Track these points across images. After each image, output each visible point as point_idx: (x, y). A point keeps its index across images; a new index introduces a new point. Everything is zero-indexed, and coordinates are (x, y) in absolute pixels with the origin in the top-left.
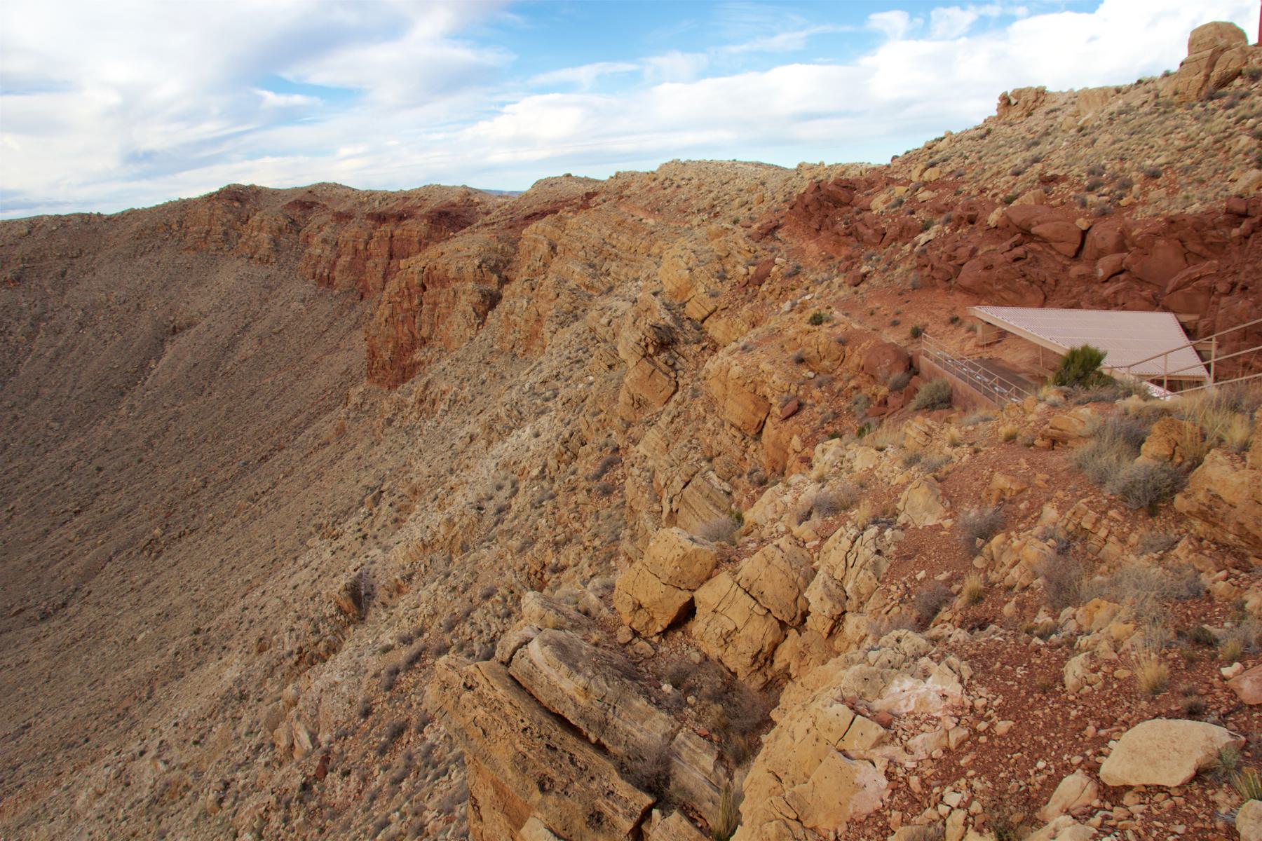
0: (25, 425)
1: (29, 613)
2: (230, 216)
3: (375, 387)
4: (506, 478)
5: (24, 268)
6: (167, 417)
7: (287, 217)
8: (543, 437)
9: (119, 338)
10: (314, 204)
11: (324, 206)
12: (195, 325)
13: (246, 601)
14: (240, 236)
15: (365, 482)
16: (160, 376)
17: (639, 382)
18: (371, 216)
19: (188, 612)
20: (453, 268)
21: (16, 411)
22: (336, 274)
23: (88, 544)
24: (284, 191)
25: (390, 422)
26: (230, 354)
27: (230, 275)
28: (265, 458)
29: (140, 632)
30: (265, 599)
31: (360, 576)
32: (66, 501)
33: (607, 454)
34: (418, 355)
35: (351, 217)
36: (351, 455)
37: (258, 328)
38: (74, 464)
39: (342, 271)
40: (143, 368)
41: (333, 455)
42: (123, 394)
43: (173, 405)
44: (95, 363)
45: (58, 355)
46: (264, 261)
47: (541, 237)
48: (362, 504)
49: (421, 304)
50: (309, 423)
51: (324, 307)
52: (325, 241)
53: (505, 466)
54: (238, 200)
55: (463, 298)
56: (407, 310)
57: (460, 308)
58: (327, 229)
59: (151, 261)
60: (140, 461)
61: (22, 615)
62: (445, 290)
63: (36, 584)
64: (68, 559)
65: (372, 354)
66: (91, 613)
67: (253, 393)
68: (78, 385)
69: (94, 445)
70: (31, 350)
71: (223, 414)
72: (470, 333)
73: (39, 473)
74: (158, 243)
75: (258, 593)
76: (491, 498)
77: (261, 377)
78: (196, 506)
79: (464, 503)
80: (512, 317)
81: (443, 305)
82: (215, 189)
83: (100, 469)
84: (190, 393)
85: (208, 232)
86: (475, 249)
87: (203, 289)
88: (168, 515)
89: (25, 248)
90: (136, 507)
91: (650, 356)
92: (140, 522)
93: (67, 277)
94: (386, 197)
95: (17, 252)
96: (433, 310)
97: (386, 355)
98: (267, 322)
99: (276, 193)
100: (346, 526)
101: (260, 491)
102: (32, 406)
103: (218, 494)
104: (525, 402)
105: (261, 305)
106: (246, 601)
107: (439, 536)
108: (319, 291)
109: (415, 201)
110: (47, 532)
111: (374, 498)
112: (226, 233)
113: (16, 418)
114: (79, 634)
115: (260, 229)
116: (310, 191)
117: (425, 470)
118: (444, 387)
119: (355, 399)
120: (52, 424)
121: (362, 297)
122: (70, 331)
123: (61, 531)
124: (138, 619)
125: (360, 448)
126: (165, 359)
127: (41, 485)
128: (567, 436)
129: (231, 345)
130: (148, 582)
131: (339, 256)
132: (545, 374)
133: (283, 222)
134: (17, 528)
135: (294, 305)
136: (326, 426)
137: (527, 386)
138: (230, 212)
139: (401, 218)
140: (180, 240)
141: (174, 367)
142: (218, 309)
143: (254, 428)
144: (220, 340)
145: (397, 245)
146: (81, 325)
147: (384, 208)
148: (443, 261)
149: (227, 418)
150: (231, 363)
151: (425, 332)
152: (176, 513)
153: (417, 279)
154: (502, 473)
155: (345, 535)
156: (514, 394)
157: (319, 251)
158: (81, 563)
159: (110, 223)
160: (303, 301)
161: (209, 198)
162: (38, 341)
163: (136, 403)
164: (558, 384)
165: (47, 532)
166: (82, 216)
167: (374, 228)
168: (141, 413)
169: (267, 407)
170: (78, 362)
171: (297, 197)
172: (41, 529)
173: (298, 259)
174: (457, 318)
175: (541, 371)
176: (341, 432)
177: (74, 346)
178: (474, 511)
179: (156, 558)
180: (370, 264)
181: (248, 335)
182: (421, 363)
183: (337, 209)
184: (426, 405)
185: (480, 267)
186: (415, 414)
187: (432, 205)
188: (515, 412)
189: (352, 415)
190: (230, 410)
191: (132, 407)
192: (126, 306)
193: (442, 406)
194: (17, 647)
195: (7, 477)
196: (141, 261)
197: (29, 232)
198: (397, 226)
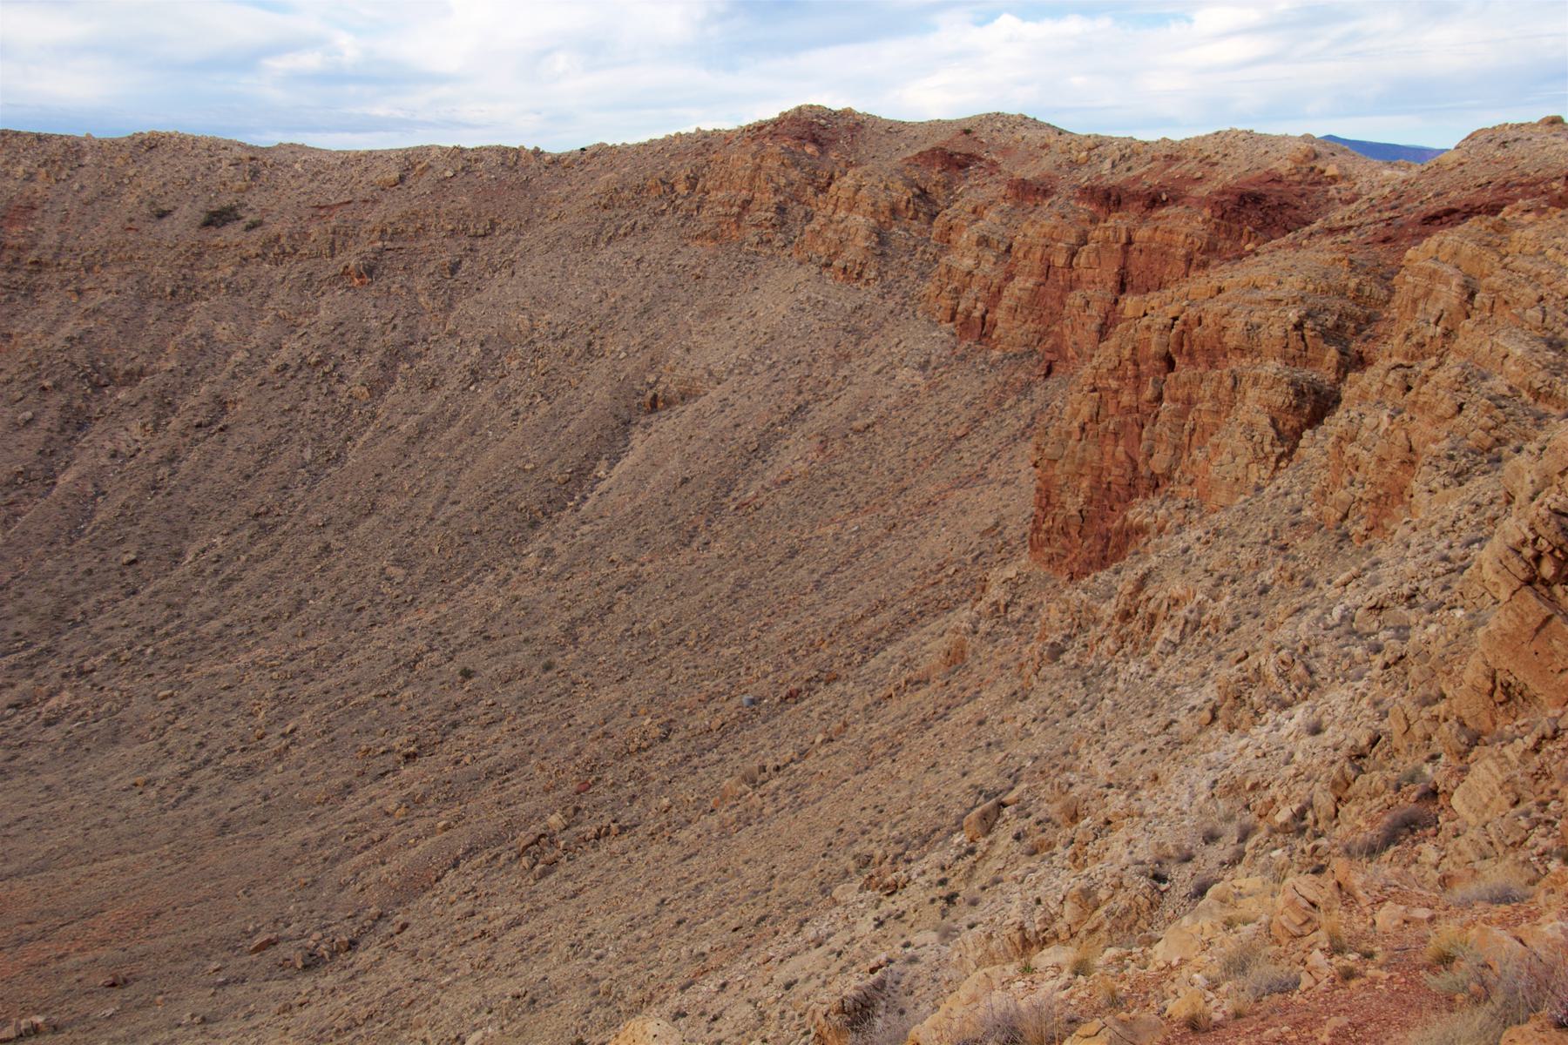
0: (342, 566)
1: (284, 951)
2: (795, 174)
3: (1042, 571)
4: (1229, 818)
5: (384, 250)
6: (613, 583)
7: (911, 183)
8: (1327, 737)
9: (544, 409)
10: (971, 158)
11: (993, 164)
12: (697, 396)
13: (686, 999)
14: (809, 217)
15: (977, 778)
16: (613, 496)
17: (1508, 640)
18: (1089, 193)
19: (575, 1001)
20: (1238, 324)
21: (329, 535)
22: (1000, 314)
23: (420, 826)
24: (912, 126)
25: (1056, 652)
26: (758, 466)
27: (780, 296)
28: (795, 695)
29: (475, 1028)
30: (723, 1000)
31: (880, 985)
32: (393, 731)
33: (1407, 803)
34: (1138, 513)
35: (1046, 193)
36: (965, 713)
37: (822, 416)
38: (419, 657)
39: (1013, 311)
40: (581, 476)
41: (929, 709)
42: (535, 525)
43: (630, 560)
44: (490, 456)
45: (422, 432)
46: (851, 274)
47: (1448, 269)
48: (959, 826)
49: (1159, 398)
50: (897, 630)
51: (966, 385)
52: (984, 241)
53: (1233, 789)
54: (815, 140)
55: (1252, 393)
56: (1129, 410)
57: (1243, 416)
58: (991, 215)
59: (625, 255)
60: (548, 667)
61: (271, 953)
62: (1214, 373)
63: (310, 893)
64: (375, 850)
65: (1046, 498)
66: (397, 971)
67: (793, 553)
68: (452, 496)
69: (464, 623)
70: (374, 417)
71: (726, 591)
72: (1258, 473)
73: (352, 666)
74: (644, 219)
75: (710, 985)
76: (1188, 858)
77: (813, 521)
78: (642, 777)
79: (1125, 859)
80: (1351, 449)
81: (1206, 405)
83: (467, 674)
84: (669, 538)
85: (746, 204)
86: (1292, 285)
87: (722, 324)
88: (584, 788)
89: (391, 209)
90: (524, 761)
91: (1547, 584)
92: (526, 794)
93: (460, 274)
94: (1130, 152)
95: (374, 217)
96: (1183, 415)
97: (1072, 504)
98: (841, 406)
99: (894, 130)
100: (916, 868)
101: (770, 764)
102: (361, 529)
103: (688, 758)
104: (1325, 649)
105: (836, 366)
106: (686, 999)
107: (1060, 926)
108: (961, 349)
109: (1190, 167)
110: (348, 788)
111: (984, 816)
112: (781, 209)
113: (327, 549)
114: (363, 1012)
115: (852, 206)
116: (967, 130)
117: (1102, 770)
118: (1177, 589)
119: (996, 593)
120: (392, 571)
121: (1049, 371)
122: (453, 383)
123: (374, 790)
124: (477, 998)
125: (988, 698)
126: (627, 462)
127: (351, 691)
128: (1364, 741)
129: (761, 449)
130: (516, 923)
131: (1010, 277)
132: (1382, 590)
133: (901, 194)
134: (294, 773)
135: (903, 374)
136: (930, 643)
137: (1337, 612)
138: (796, 164)
139: (1154, 201)
140: (688, 217)
141: (642, 481)
142: (746, 367)
143: (783, 627)
144: (741, 434)
145: (1138, 261)
146: (475, 375)
147: (1120, 178)
148: (1216, 307)
149: (733, 599)
150: (756, 485)
151: (1159, 463)
152: (600, 787)
153: (1155, 344)
154: (1223, 806)
155: (911, 888)
156: (1303, 626)
157: (968, 262)
158: (397, 862)
159: (557, 170)
160: (923, 367)
161: (757, 132)
162: (389, 398)
163: (558, 546)
164: (1411, 616)
165: (348, 788)
166: (504, 151)
167: (1094, 220)
168: (565, 568)
169: (818, 585)
170: (459, 451)
171: (939, 140)
172: (337, 782)
173: (923, 276)
174: (1232, 439)
175: (1375, 582)
176: (956, 659)
177: (455, 416)
178: (1144, 882)
179: (544, 874)
180: (1075, 299)
181: (801, 428)
182: (1141, 530)
183: (1019, 173)
184: (1135, 626)
185: (1299, 326)
186: (1109, 642)
187: (1228, 176)
188: (1299, 669)
189: (984, 627)
190: (741, 584)
191: (548, 553)
192: (566, 344)
193: (1166, 632)
194: (248, 1016)
195: (292, 667)
196: (607, 253)
197: (402, 179)
198: (1143, 219)
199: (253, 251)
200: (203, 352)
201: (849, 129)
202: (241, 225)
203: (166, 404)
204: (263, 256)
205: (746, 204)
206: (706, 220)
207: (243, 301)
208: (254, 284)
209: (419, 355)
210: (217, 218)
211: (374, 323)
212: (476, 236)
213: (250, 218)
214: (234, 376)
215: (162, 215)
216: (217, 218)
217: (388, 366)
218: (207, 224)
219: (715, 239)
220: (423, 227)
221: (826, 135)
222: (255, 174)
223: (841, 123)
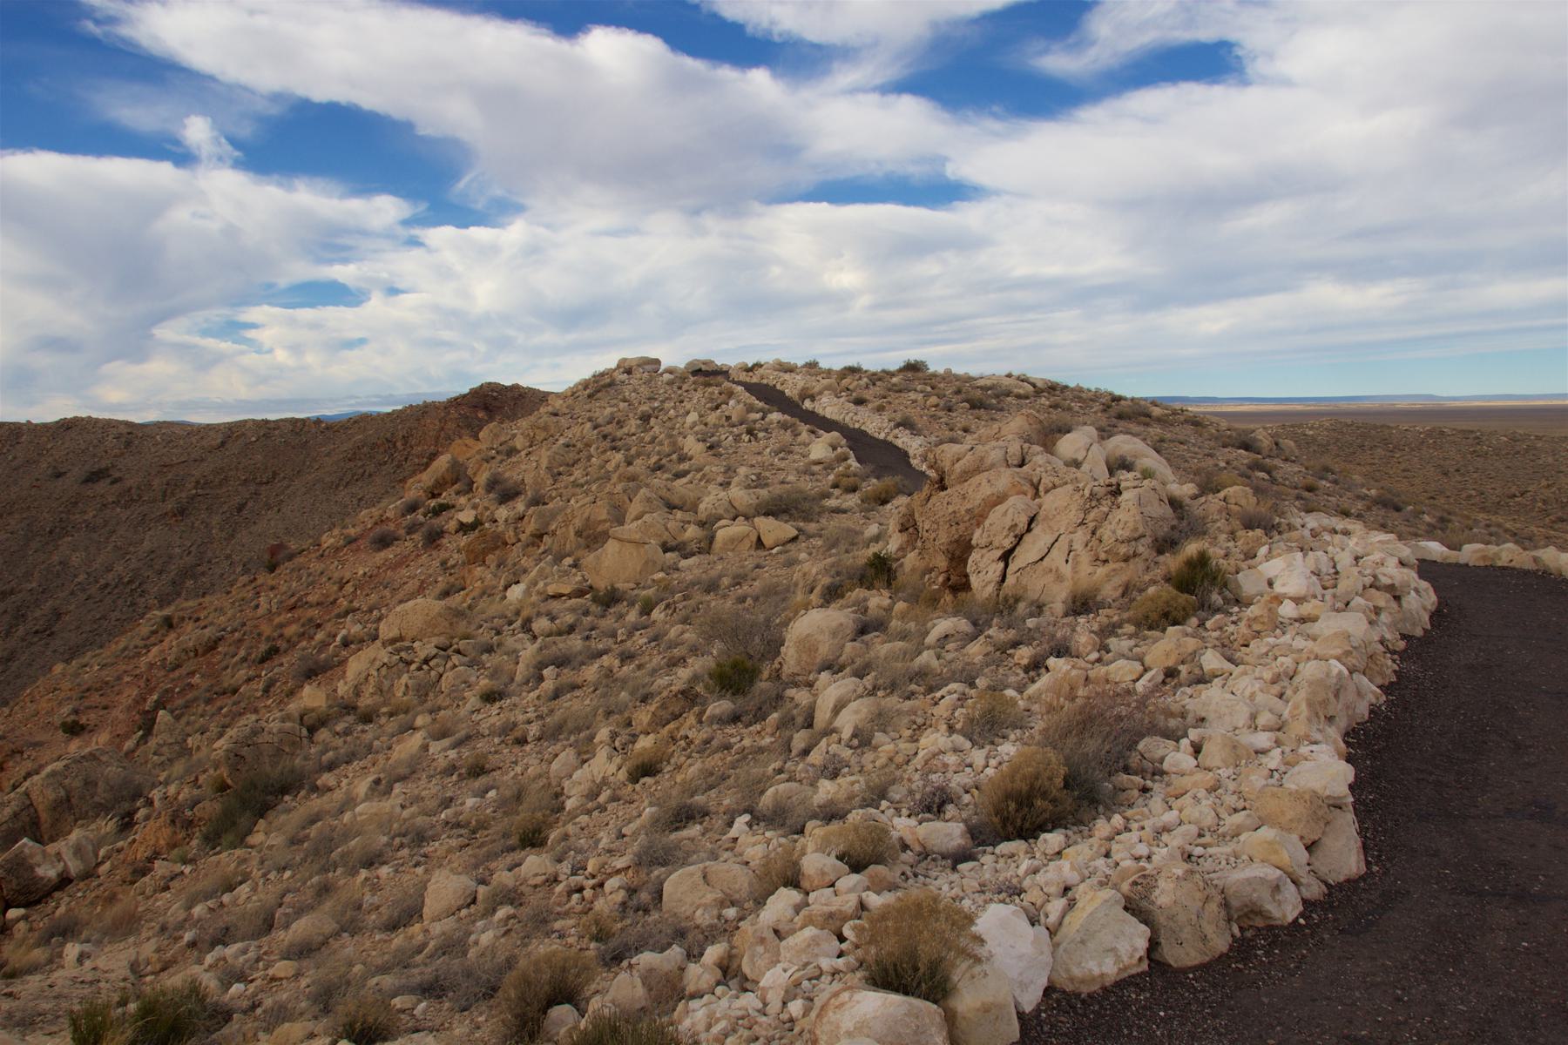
5: (193, 498)
54: (486, 408)
59: (353, 495)
74: (370, 468)
161: (457, 402)
166: (294, 421)
197: (223, 443)
200: (58, 575)
201: (514, 398)
202: (108, 480)
203: (20, 616)
204: (116, 503)
207: (95, 536)
208: (106, 523)
209: (203, 574)
210: (94, 477)
211: (177, 550)
213: (117, 475)
214: (72, 593)
215: (59, 475)
216: (94, 477)
218: (87, 481)
220: (226, 479)
221: (497, 404)
222: (128, 444)
223: (509, 394)
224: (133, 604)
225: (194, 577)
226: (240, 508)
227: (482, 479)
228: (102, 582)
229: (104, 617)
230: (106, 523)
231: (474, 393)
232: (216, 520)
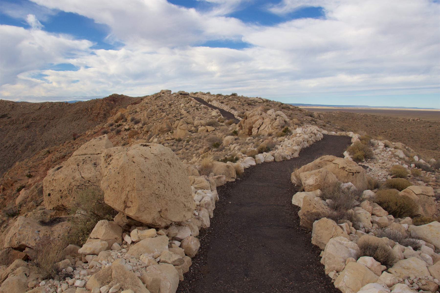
2: (108, 107)
5: (31, 123)
54: (114, 101)
59: (76, 124)
74: (81, 116)
82: (108, 95)
85: (99, 114)
112: (105, 115)
138: (109, 106)
140: (89, 116)
161: (106, 99)
162: (25, 153)
166: (60, 103)
192: (60, 142)
196: (73, 123)
197: (40, 108)
199: (7, 123)
204: (9, 124)
205: (99, 114)
206: (92, 116)
207: (3, 133)
208: (6, 129)
209: (34, 144)
211: (27, 137)
212: (51, 120)
213: (10, 116)
217: (26, 147)
219: (92, 120)
220: (41, 118)
222: (13, 108)
223: (120, 97)
224: (14, 152)
225: (31, 145)
226: (45, 126)
227: (129, 118)
228: (5, 146)
229: (6, 155)
230: (6, 129)
231: (110, 96)
232: (37, 129)
